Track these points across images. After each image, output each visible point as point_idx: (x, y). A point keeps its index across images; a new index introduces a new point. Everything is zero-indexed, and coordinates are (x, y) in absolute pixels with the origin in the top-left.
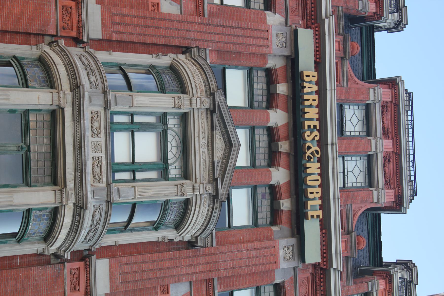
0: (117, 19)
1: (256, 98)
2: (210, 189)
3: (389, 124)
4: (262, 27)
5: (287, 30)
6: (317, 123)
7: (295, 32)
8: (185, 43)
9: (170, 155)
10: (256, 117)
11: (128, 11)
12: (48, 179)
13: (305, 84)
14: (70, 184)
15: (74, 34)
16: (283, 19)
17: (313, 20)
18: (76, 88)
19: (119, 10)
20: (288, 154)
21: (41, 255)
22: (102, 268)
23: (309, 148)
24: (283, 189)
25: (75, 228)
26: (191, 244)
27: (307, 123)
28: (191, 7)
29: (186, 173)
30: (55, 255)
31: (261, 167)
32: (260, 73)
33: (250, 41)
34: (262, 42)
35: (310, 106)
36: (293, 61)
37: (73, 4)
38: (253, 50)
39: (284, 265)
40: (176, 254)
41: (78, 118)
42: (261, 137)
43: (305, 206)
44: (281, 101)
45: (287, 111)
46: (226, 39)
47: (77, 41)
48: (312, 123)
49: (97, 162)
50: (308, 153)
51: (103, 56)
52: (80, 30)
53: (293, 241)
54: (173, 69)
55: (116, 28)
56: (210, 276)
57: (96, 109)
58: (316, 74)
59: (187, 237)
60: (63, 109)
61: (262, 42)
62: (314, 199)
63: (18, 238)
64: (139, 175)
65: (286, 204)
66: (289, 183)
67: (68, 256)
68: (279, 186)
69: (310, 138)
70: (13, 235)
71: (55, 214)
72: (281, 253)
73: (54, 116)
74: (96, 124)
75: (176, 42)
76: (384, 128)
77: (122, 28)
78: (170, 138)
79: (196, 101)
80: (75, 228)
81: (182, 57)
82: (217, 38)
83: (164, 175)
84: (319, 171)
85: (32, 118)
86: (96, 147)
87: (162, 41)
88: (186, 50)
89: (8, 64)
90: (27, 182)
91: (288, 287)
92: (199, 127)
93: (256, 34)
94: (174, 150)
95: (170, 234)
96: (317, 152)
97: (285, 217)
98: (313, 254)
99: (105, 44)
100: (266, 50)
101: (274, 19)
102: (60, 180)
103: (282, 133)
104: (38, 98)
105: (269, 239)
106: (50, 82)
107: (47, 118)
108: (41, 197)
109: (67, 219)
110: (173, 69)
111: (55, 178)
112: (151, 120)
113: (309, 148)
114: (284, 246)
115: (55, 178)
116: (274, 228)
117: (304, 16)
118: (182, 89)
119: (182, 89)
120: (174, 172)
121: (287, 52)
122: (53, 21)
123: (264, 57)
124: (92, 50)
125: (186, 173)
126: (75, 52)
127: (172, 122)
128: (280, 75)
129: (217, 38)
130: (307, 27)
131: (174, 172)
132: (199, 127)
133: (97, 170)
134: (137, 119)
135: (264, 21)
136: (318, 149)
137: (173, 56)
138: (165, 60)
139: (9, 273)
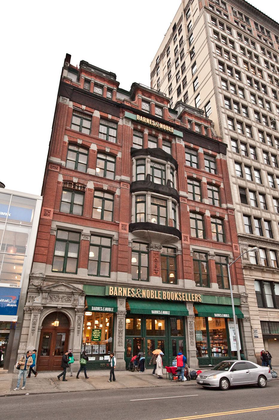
3: (147, 95)
13: (141, 120)
23: (156, 125)
24: (164, 137)
27: (150, 123)
29: (164, 165)
33: (128, 133)
36: (133, 121)
48: (150, 122)
50: (158, 126)
54: (137, 160)
60: (152, 194)
62: (169, 128)
65: (168, 137)
68: (163, 137)
76: (149, 97)
84: (162, 124)
93: (126, 130)
94: (158, 166)
96: (157, 123)
98: (180, 134)
99: (131, 177)
101: (121, 122)
102: (166, 199)
113: (156, 125)
125: (164, 165)
136: (157, 122)
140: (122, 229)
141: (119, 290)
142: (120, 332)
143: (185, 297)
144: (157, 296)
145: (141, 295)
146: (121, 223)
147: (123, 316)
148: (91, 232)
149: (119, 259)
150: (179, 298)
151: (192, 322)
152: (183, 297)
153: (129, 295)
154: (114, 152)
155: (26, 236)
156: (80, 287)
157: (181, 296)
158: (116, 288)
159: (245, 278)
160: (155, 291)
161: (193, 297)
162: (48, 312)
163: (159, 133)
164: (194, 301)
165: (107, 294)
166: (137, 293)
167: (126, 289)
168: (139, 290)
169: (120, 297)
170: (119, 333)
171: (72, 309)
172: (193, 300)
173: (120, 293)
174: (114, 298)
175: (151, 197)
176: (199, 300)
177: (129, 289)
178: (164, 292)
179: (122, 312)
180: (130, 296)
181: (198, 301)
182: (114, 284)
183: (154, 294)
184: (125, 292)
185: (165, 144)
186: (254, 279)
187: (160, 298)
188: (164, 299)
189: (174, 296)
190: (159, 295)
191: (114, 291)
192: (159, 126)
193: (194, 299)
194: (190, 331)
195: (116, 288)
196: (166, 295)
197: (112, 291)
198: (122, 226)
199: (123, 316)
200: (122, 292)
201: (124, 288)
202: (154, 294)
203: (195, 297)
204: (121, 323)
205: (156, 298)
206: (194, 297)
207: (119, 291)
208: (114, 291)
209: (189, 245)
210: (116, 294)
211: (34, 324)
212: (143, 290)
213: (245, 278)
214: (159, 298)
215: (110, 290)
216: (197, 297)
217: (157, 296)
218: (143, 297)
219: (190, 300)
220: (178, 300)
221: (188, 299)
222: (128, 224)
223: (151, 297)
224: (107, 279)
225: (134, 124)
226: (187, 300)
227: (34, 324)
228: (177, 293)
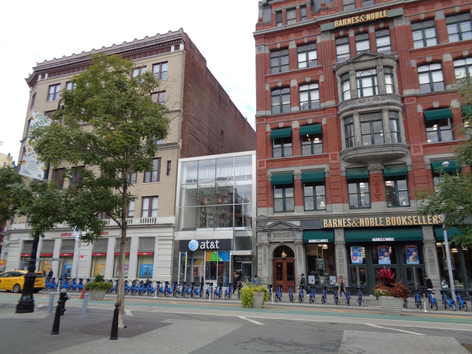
0: (328, 96)
1: (345, 42)
2: (379, 60)
4: (322, 45)
5: (322, 35)
6: (353, 18)
7: (323, 32)
8: (332, 72)
9: (369, 74)
10: (352, 41)
11: (325, 91)
12: (380, 114)
14: (381, 108)
15: (335, 109)
16: (318, 36)
17: (317, 25)
18: (352, 109)
19: (326, 96)
20: (364, 27)
21: (402, 112)
22: (406, 92)
23: (361, 20)
25: (394, 104)
26: (398, 61)
27: (353, 23)
28: (320, 72)
30: (402, 108)
31: (369, 36)
32: (337, 41)
34: (327, 44)
35: (347, 22)
36: (332, 31)
37: (326, 110)
38: (330, 47)
39: (405, 22)
40: (401, 66)
41: (361, 107)
42: (359, 37)
43: (382, 18)
44: (346, 33)
45: (348, 30)
46: (328, 57)
47: (337, 108)
48: (353, 20)
49: (374, 100)
51: (340, 100)
52: (333, 107)
53: (395, 21)
54: (341, 76)
55: (331, 96)
56: (408, 53)
57: (357, 102)
58: (335, 22)
59: (395, 63)
61: (327, 44)
63: (397, 120)
64: (376, 84)
66: (374, 25)
67: (403, 104)
69: (358, 20)
70: (397, 122)
71: (390, 111)
72: (399, 25)
73: (361, 114)
74: (362, 101)
75: (332, 75)
77: (331, 94)
78: (363, 75)
79: (351, 67)
80: (394, 104)
81: (337, 73)
82: (329, 61)
83: (376, 75)
85: (362, 120)
86: (369, 100)
87: (333, 80)
88: (334, 72)
89: (346, 128)
90: (381, 120)
91: (412, 19)
92: (359, 66)
93: (325, 46)
94: (367, 73)
95: (394, 70)
97: (387, 25)
98: (399, 11)
99: (337, 99)
100: (330, 42)
103: (357, 31)
104: (356, 119)
105: (394, 29)
106: (351, 116)
107: (361, 116)
108: (386, 116)
109: (392, 107)
110: (341, 76)
111: (380, 111)
112: (358, 82)
113: (361, 20)
114: (397, 24)
115: (380, 111)
116: (390, 28)
117: (316, 28)
118: (348, 73)
119: (348, 73)
120: (374, 72)
121: (329, 34)
122: (332, 116)
123: (332, 41)
124: (339, 103)
126: (341, 109)
127: (358, 74)
128: (337, 34)
129: (329, 61)
130: (319, 26)
131: (374, 72)
132: (359, 66)
133: (376, 99)
134: (359, 87)
135: (321, 43)
137: (337, 76)
138: (339, 79)
139: (408, 122)
140: (332, 159)
141: (334, 221)
142: (341, 261)
144: (378, 223)
146: (330, 154)
147: (342, 246)
148: (301, 170)
149: (332, 191)
151: (432, 248)
152: (414, 220)
153: (344, 226)
154: (314, 79)
155: (250, 186)
156: (297, 223)
157: (412, 219)
158: (330, 220)
160: (376, 219)
162: (274, 247)
163: (368, 26)
164: (431, 223)
165: (322, 227)
166: (354, 222)
167: (341, 220)
168: (355, 219)
169: (337, 228)
170: (340, 262)
171: (293, 242)
172: (430, 223)
173: (335, 225)
174: (331, 230)
177: (344, 220)
178: (387, 218)
179: (340, 242)
180: (346, 226)
182: (328, 217)
183: (374, 221)
184: (341, 223)
185: (381, 35)
187: (383, 225)
188: (387, 225)
189: (403, 221)
190: (381, 222)
191: (328, 223)
192: (365, 19)
193: (431, 221)
194: (430, 258)
195: (330, 220)
196: (391, 221)
197: (326, 224)
198: (332, 157)
200: (337, 223)
201: (339, 220)
202: (374, 221)
204: (340, 252)
205: (377, 225)
207: (334, 223)
208: (328, 223)
209: (422, 156)
210: (330, 225)
211: (265, 256)
212: (360, 219)
214: (381, 225)
215: (325, 223)
217: (378, 223)
218: (361, 226)
219: (425, 223)
220: (407, 224)
222: (338, 153)
223: (371, 225)
224: (323, 213)
225: (334, 33)
226: (420, 223)
227: (265, 256)
228: (405, 217)
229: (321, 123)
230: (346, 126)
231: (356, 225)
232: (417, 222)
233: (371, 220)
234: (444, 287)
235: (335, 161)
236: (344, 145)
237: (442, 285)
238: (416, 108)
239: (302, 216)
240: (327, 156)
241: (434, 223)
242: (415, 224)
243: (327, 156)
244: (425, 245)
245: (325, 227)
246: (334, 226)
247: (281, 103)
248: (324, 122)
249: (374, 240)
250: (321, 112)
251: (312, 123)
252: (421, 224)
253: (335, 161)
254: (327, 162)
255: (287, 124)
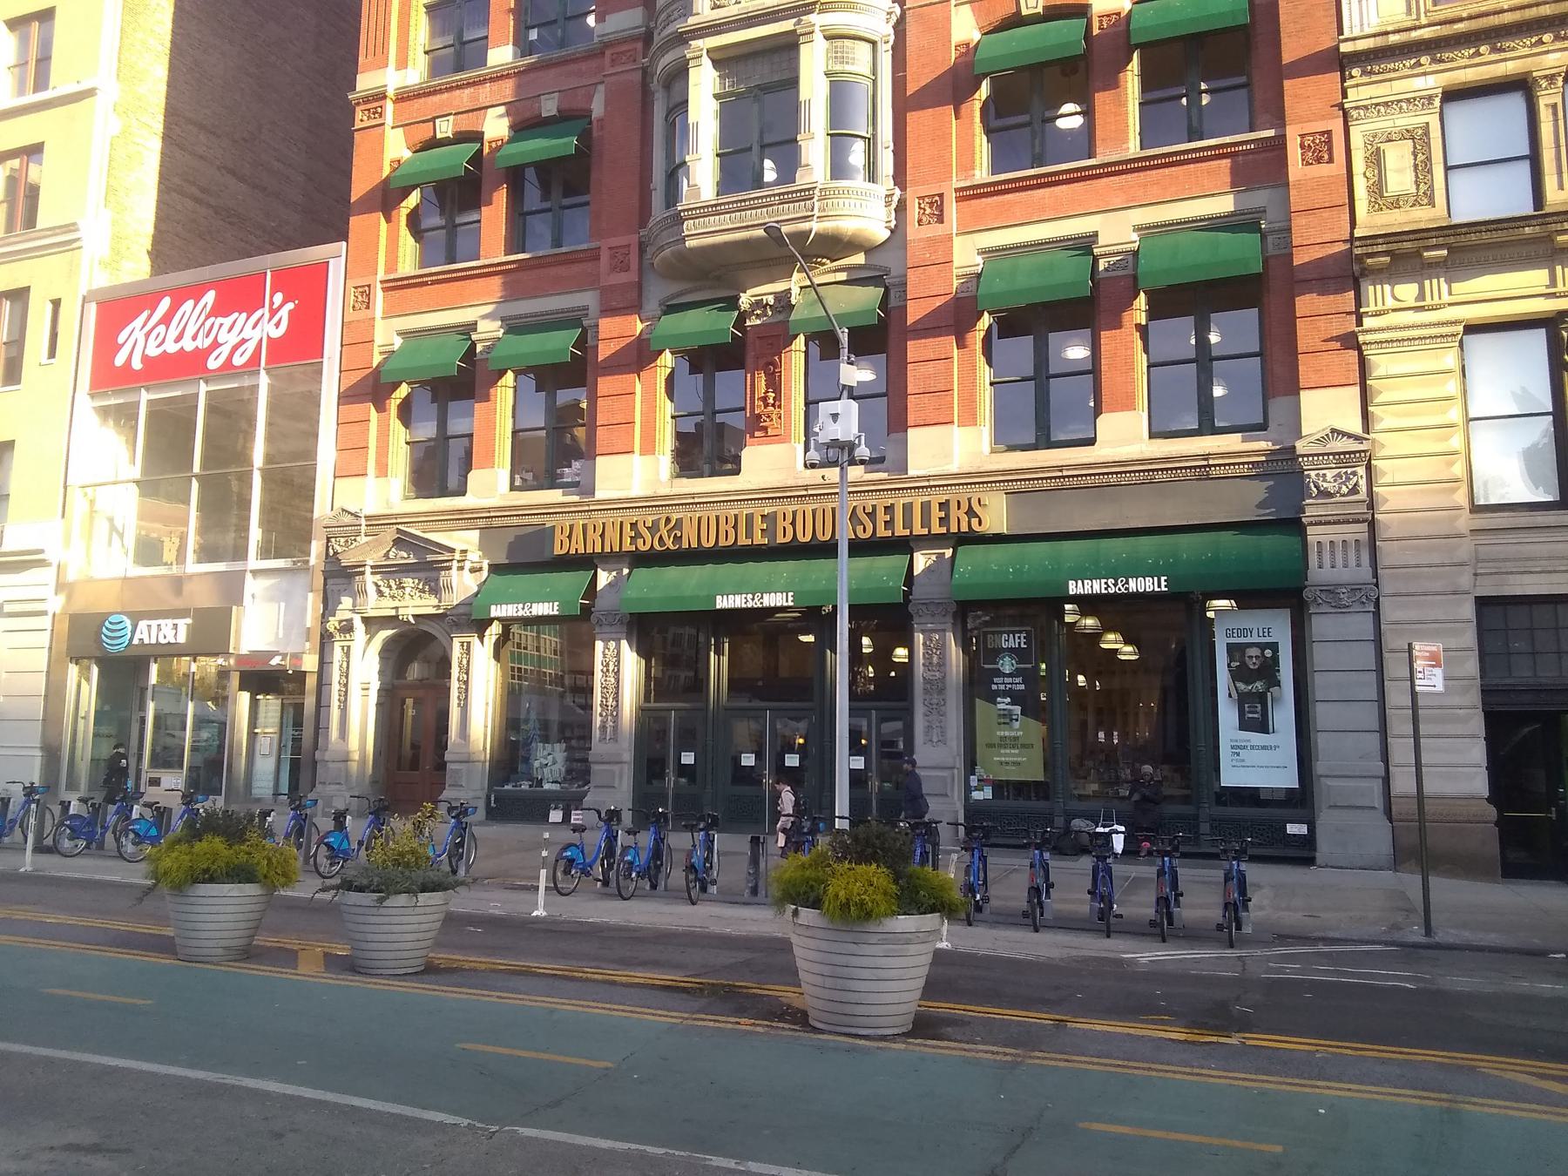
15: (639, 45)
37: (608, 53)
47: (647, 38)
52: (634, 39)
102: (790, 39)
140: (613, 269)
143: (892, 519)
144: (749, 534)
145: (678, 539)
150: (860, 529)
152: (882, 517)
153: (628, 546)
157: (872, 515)
159: (1369, 337)
161: (936, 513)
165: (547, 556)
172: (937, 529)
175: (717, 64)
176: (975, 521)
181: (964, 528)
186: (1455, 323)
188: (780, 540)
191: (570, 537)
196: (793, 523)
198: (613, 257)
199: (613, 629)
200: (602, 536)
203: (947, 515)
205: (743, 541)
206: (943, 514)
213: (1369, 337)
214: (759, 539)
216: (965, 507)
217: (749, 534)
219: (918, 530)
221: (908, 523)
222: (633, 239)
226: (900, 531)
229: (587, 114)
230: (670, 112)
231: (670, 544)
232: (889, 524)
233: (722, 521)
234: (977, 795)
235: (622, 278)
236: (657, 199)
237: (968, 789)
238: (948, 19)
239: (488, 510)
240: (594, 256)
241: (954, 529)
242: (882, 532)
243: (594, 256)
244: (916, 619)
245: (558, 551)
246: (590, 551)
247: (460, 35)
248: (598, 108)
249: (722, 603)
250: (593, 64)
251: (554, 112)
252: (907, 532)
253: (622, 278)
254: (590, 282)
255: (466, 124)
